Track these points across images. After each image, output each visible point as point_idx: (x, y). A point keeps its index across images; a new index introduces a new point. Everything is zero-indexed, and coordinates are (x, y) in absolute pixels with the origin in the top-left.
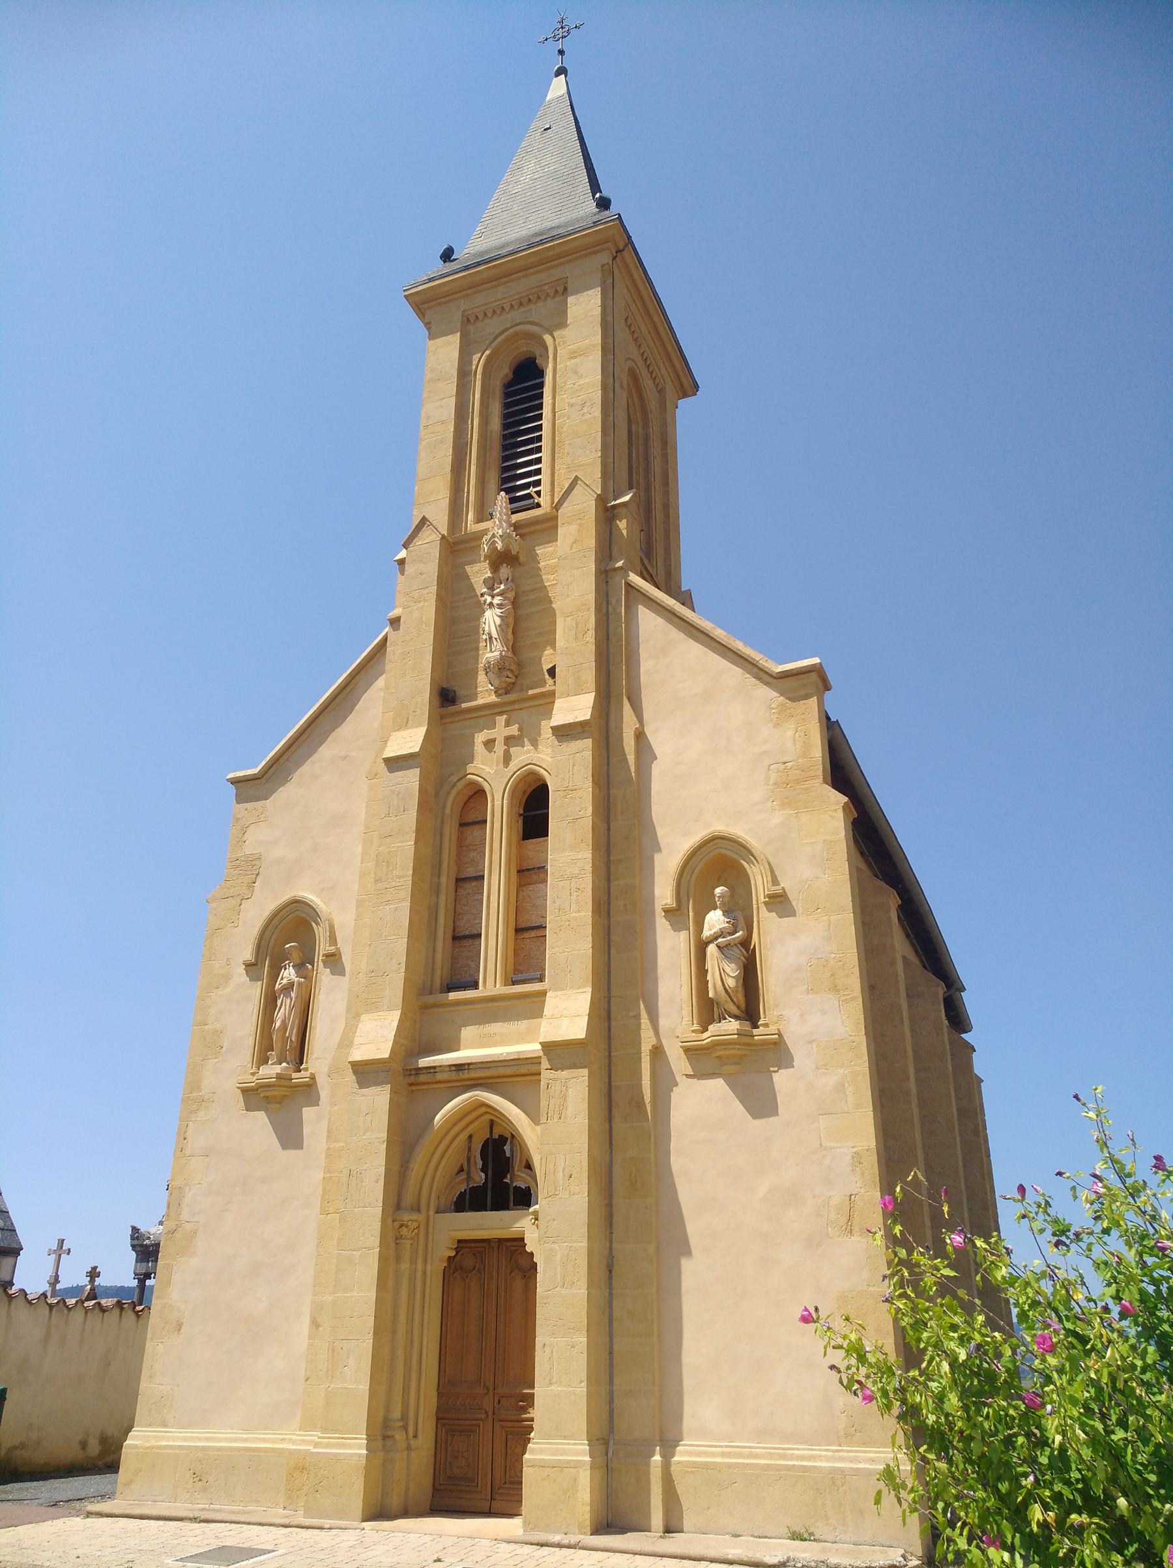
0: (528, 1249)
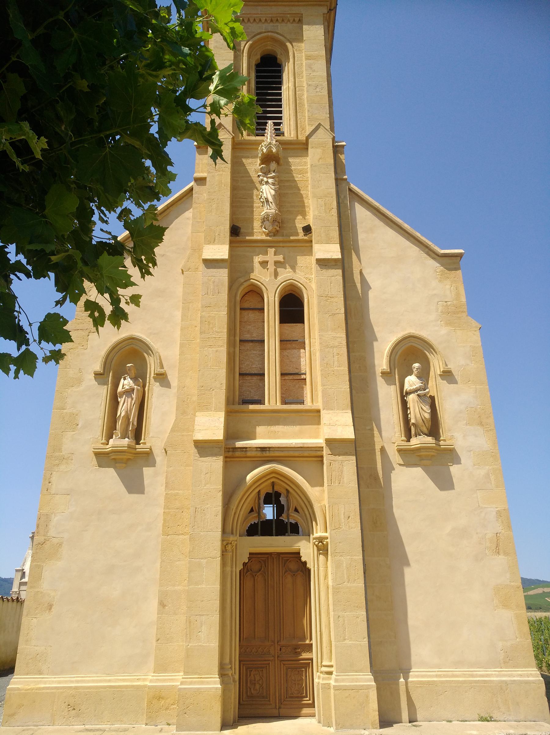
0: (303, 559)
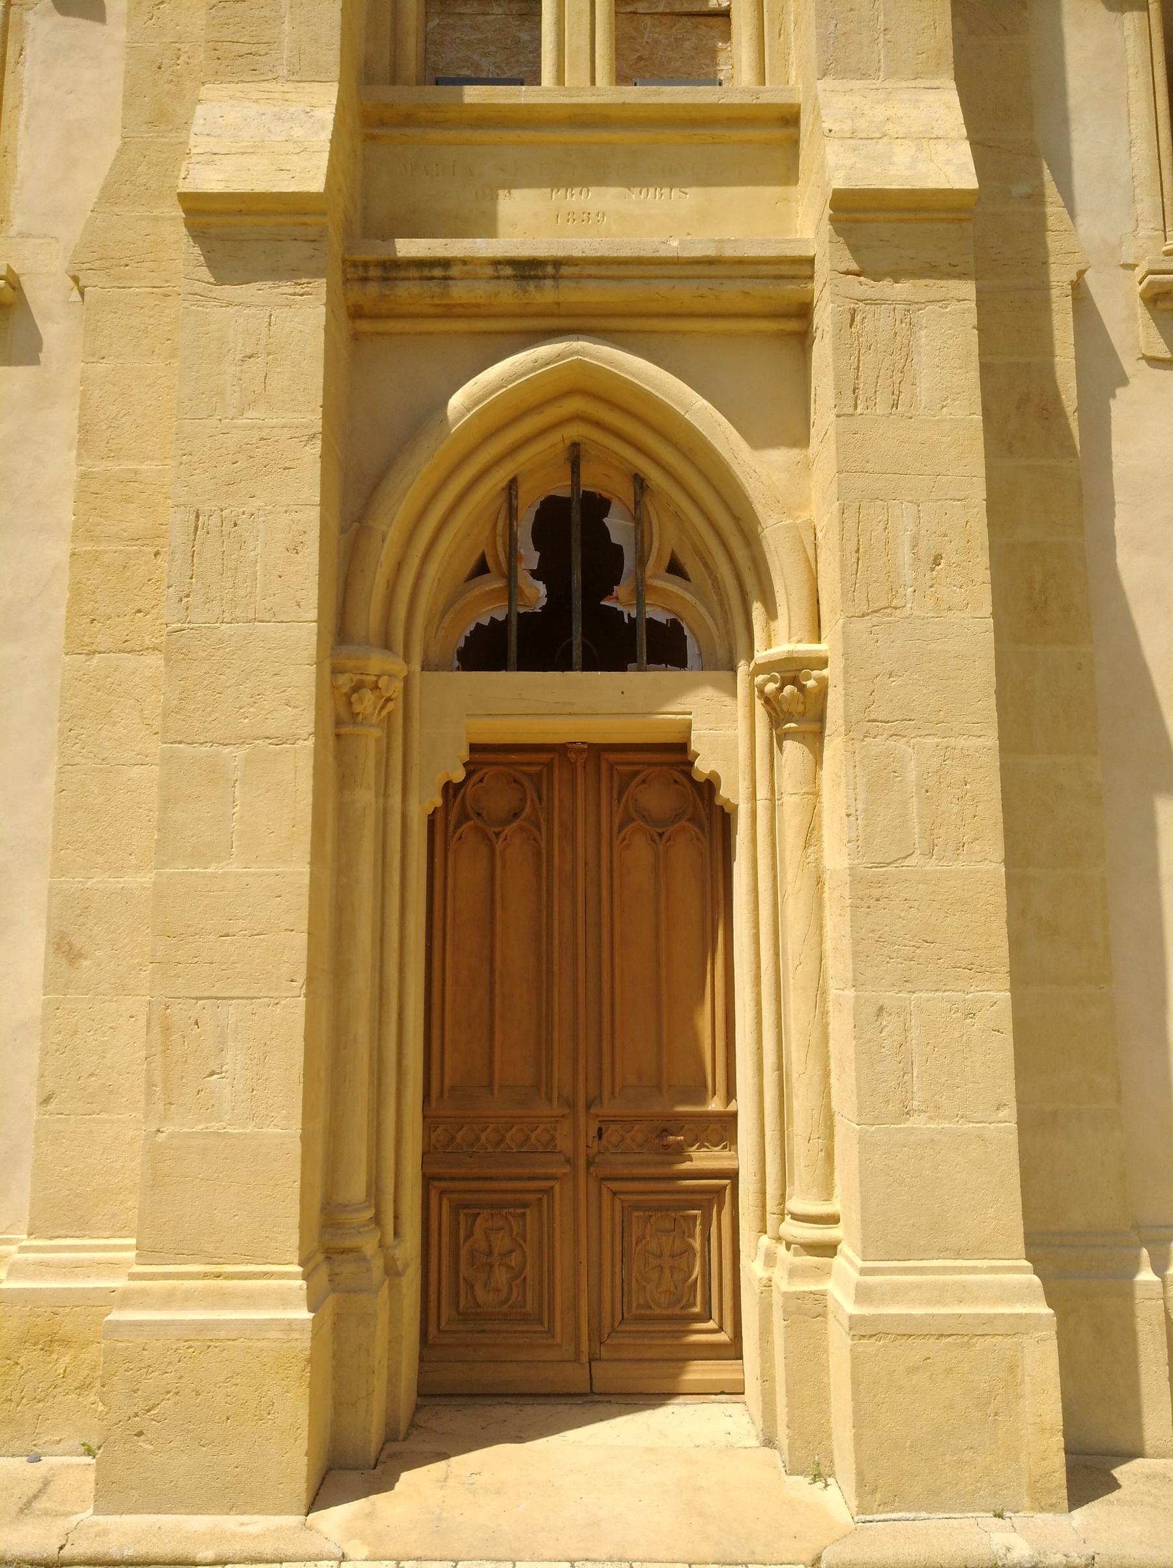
0: (703, 766)
